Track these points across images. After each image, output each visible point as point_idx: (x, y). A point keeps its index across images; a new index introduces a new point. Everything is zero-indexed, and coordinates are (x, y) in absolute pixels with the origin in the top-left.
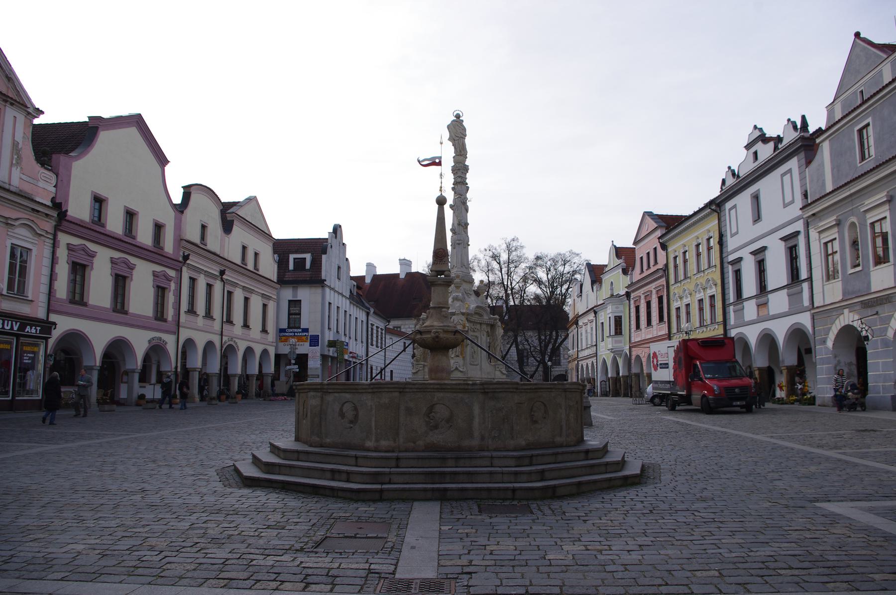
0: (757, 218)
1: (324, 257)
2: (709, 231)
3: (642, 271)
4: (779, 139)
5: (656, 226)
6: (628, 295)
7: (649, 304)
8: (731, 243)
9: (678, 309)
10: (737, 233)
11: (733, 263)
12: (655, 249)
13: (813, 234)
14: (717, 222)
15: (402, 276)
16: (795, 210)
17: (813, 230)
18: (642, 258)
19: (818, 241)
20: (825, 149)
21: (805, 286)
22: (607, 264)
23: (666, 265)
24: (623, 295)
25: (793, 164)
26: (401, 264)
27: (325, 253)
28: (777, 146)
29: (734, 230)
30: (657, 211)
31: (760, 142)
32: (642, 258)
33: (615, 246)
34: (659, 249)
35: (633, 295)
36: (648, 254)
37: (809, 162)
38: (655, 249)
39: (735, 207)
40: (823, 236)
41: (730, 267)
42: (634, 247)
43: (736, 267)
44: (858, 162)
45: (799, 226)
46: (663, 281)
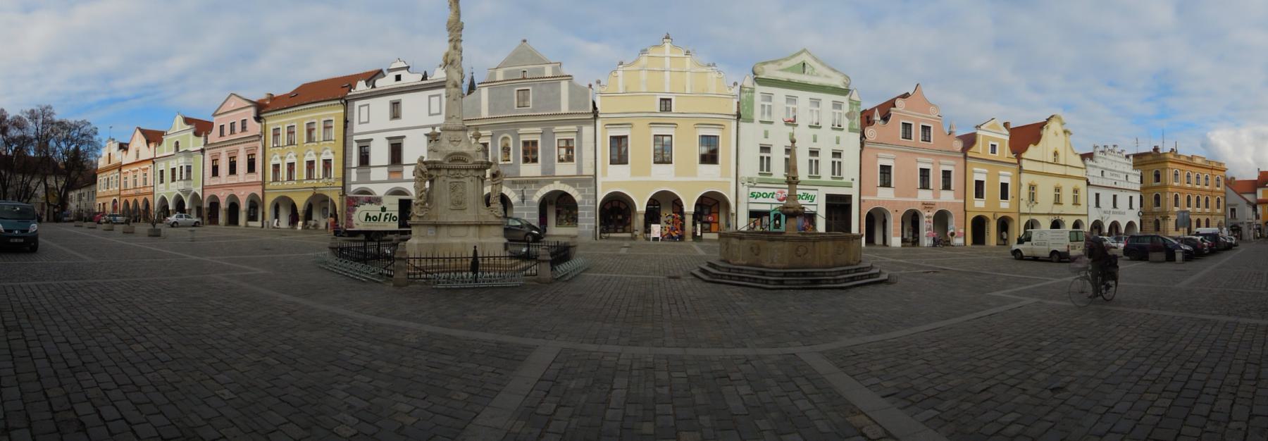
3: (222, 134)
8: (357, 128)
9: (276, 167)
10: (368, 122)
11: (357, 141)
12: (244, 122)
14: (343, 111)
18: (222, 127)
23: (264, 132)
32: (222, 127)
36: (232, 125)
38: (244, 122)
39: (368, 105)
46: (260, 144)
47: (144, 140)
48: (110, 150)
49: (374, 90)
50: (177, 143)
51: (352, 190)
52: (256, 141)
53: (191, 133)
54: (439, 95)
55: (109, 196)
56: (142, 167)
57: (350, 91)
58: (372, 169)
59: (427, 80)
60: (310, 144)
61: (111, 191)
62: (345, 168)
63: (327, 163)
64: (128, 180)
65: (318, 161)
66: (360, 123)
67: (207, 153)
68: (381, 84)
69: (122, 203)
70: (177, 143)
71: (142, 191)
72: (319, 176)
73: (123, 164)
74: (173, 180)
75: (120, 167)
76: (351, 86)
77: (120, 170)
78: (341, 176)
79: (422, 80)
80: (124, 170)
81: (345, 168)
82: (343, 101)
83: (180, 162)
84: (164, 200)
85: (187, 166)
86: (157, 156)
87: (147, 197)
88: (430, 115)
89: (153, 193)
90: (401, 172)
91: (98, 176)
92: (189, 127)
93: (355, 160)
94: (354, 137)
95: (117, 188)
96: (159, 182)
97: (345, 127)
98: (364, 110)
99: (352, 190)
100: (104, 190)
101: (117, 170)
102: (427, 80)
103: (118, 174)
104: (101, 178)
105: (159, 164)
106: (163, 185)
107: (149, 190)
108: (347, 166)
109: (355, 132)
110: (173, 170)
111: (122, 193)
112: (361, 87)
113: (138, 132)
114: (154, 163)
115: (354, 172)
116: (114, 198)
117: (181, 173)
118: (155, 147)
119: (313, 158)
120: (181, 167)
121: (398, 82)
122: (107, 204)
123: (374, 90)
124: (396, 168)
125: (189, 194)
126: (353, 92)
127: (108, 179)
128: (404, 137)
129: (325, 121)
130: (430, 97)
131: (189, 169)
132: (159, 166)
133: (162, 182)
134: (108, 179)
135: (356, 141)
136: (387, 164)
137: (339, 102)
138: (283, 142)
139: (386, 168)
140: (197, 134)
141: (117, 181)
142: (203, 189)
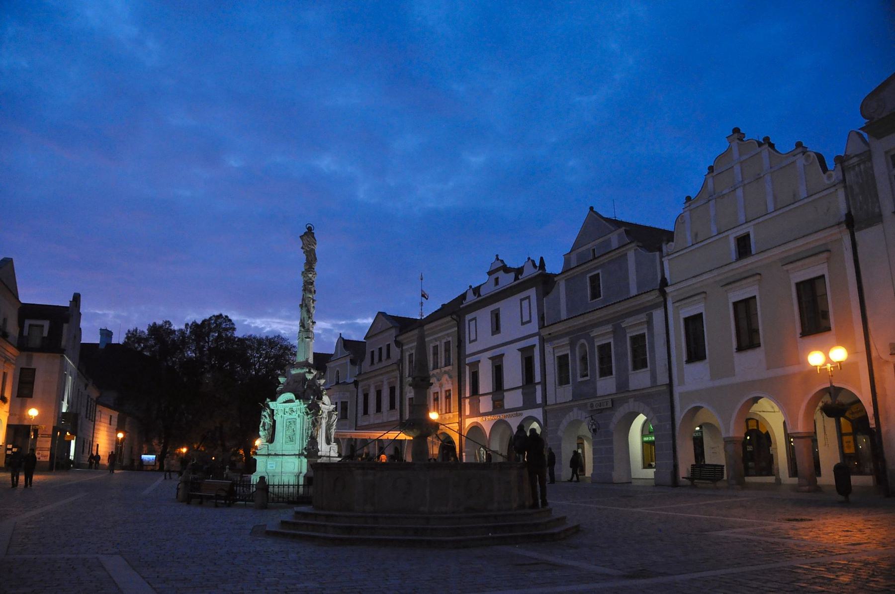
0: (496, 328)
1: (65, 326)
2: (448, 335)
4: (519, 271)
5: (391, 326)
6: (356, 383)
7: (379, 393)
8: (470, 348)
10: (476, 340)
11: (470, 365)
13: (548, 348)
15: (102, 347)
16: (534, 327)
19: (552, 355)
20: (562, 288)
21: (539, 388)
22: (333, 353)
24: (351, 383)
25: (532, 292)
26: (101, 334)
27: (67, 322)
28: (518, 276)
29: (473, 337)
30: (390, 313)
31: (502, 271)
33: (343, 339)
35: (360, 385)
37: (546, 293)
39: (475, 319)
41: (467, 368)
42: (365, 341)
44: (589, 300)
45: (535, 341)
49: (480, 298)
57: (462, 304)
58: (505, 393)
65: (441, 392)
66: (470, 342)
82: (455, 317)
88: (523, 324)
94: (467, 359)
108: (463, 396)
109: (467, 353)
121: (498, 287)
123: (480, 298)
126: (466, 303)
136: (521, 385)
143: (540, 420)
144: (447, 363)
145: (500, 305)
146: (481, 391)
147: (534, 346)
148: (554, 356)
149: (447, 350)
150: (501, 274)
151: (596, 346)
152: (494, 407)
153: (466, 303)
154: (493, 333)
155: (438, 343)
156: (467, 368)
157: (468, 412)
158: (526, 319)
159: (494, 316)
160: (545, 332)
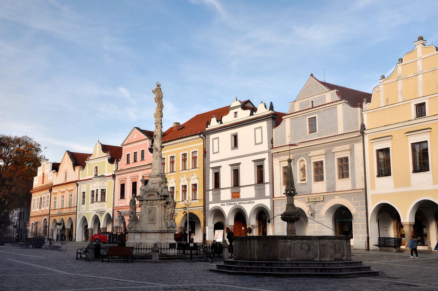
2: (196, 147)
3: (128, 162)
8: (212, 157)
10: (218, 152)
11: (213, 168)
12: (143, 151)
13: (276, 161)
14: (203, 144)
16: (265, 146)
17: (277, 159)
18: (128, 155)
29: (216, 150)
32: (128, 155)
34: (147, 152)
36: (135, 153)
38: (143, 151)
39: (218, 138)
40: (282, 163)
41: (211, 171)
43: (216, 171)
45: (266, 156)
47: (71, 163)
48: (44, 169)
49: (222, 125)
50: (96, 167)
51: (210, 208)
52: (149, 168)
53: (106, 160)
54: (261, 127)
55: (41, 216)
56: (69, 189)
57: (208, 127)
59: (253, 115)
60: (184, 171)
61: (42, 211)
62: (205, 191)
63: (195, 185)
64: (57, 200)
65: (189, 185)
66: (214, 153)
67: (117, 177)
68: (227, 119)
69: (51, 222)
70: (96, 167)
71: (64, 211)
72: (189, 198)
73: (54, 184)
74: (93, 202)
75: (50, 188)
76: (208, 123)
77: (51, 190)
78: (202, 197)
79: (250, 115)
80: (54, 190)
81: (205, 191)
82: (202, 136)
83: (97, 185)
84: (85, 220)
85: (102, 190)
86: (81, 179)
87: (71, 216)
88: (256, 144)
89: (75, 213)
90: (239, 193)
91: (33, 195)
92: (105, 154)
93: (211, 185)
95: (48, 208)
96: (81, 203)
97: (205, 156)
98: (216, 141)
99: (210, 208)
100: (37, 210)
101: (48, 191)
102: (253, 115)
103: (49, 194)
104: (35, 197)
105: (82, 187)
106: (84, 206)
107: (73, 210)
109: (211, 160)
110: (93, 191)
111: (52, 213)
112: (214, 124)
113: (67, 156)
114: (77, 185)
115: (211, 193)
116: (45, 217)
117: (97, 195)
118: (80, 171)
119: (185, 183)
120: (97, 190)
121: (236, 118)
122: (38, 224)
124: (236, 190)
125: (103, 214)
126: (210, 127)
127: (41, 198)
128: (240, 163)
129: (193, 152)
130: (255, 129)
131: (103, 192)
132: (82, 189)
133: (84, 203)
134: (41, 198)
135: (212, 168)
137: (198, 136)
138: (167, 170)
139: (230, 190)
140: (111, 161)
141: (48, 201)
142: (113, 210)
143: (269, 208)
144: (195, 167)
145: (239, 131)
146: (222, 185)
147: (264, 159)
148: (280, 167)
149: (194, 158)
150: (239, 110)
151: (312, 162)
152: (233, 197)
153: (210, 127)
154: (232, 149)
155: (187, 152)
156: (211, 171)
157: (211, 199)
158: (259, 140)
159: (233, 138)
160: (273, 151)
